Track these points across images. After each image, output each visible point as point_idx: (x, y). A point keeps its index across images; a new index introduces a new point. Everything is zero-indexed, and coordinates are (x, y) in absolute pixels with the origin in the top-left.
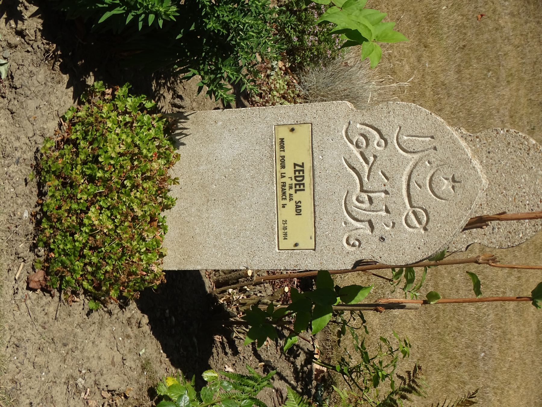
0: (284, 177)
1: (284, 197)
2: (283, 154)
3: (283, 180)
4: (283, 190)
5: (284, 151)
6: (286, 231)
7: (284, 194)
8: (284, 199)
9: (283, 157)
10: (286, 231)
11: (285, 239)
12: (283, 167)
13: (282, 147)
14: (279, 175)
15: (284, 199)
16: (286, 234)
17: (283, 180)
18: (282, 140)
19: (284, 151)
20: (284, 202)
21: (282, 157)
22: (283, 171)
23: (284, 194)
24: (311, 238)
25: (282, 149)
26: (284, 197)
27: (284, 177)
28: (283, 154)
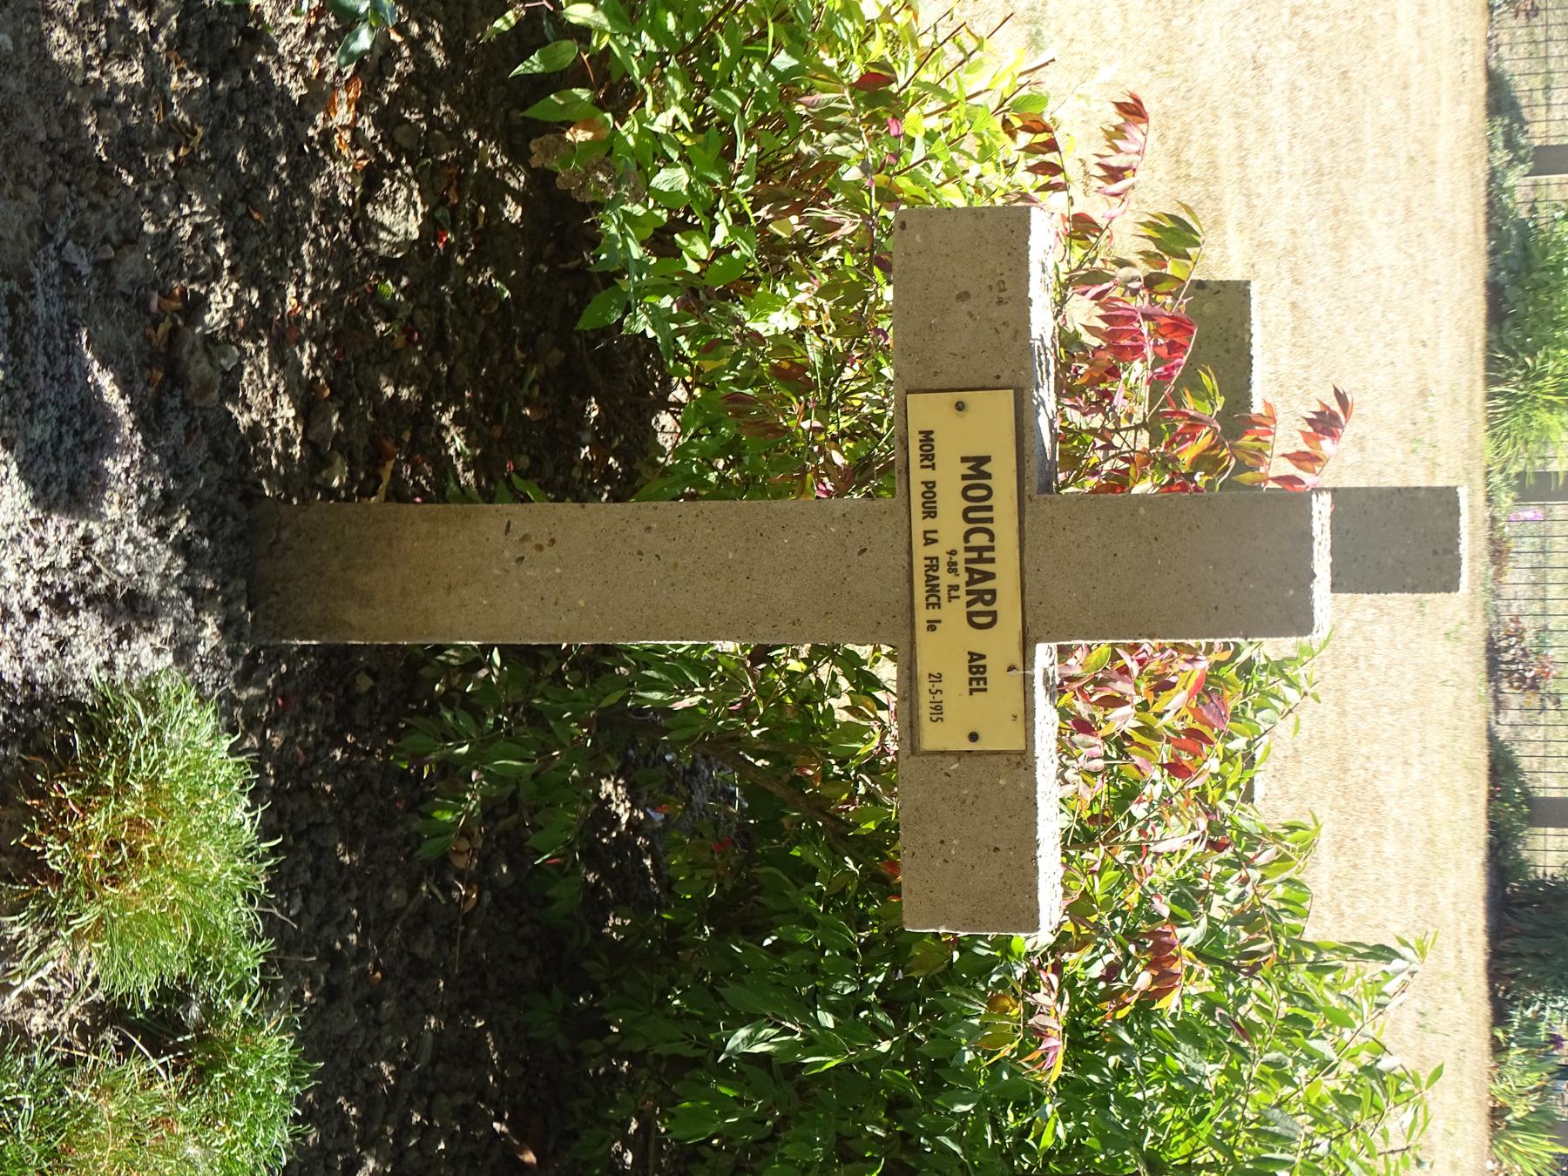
0: (935, 541)
1: (933, 600)
2: (928, 475)
3: (932, 550)
4: (930, 579)
5: (933, 467)
6: (938, 697)
7: (933, 589)
8: (933, 605)
9: (930, 486)
10: (938, 697)
12: (930, 513)
13: (928, 456)
15: (933, 605)
16: (938, 708)
17: (932, 550)
18: (927, 437)
19: (933, 467)
20: (933, 614)
22: (930, 524)
23: (933, 589)
25: (926, 463)
26: (933, 600)
27: (935, 541)
28: (928, 475)
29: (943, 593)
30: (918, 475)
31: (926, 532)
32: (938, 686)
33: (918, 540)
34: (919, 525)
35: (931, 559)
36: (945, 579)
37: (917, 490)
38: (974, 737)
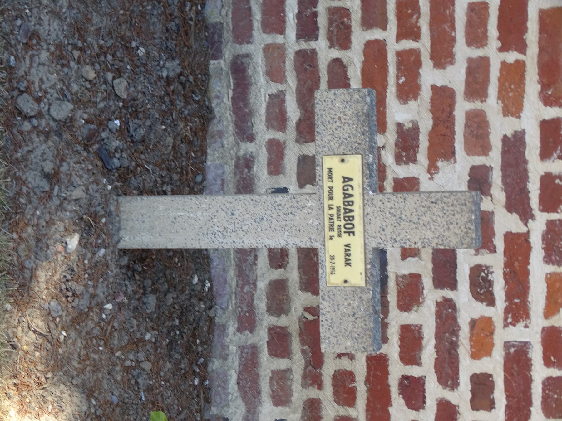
0: (332, 208)
2: (330, 184)
3: (331, 212)
6: (333, 265)
9: (331, 188)
10: (333, 265)
11: (332, 273)
12: (331, 198)
13: (330, 177)
14: (326, 208)
16: (333, 268)
17: (331, 212)
18: (330, 170)
19: (332, 181)
21: (329, 187)
22: (331, 202)
24: (361, 274)
25: (330, 180)
27: (332, 208)
28: (330, 184)
29: (335, 227)
30: (327, 185)
31: (329, 205)
32: (333, 261)
33: (326, 208)
34: (326, 202)
35: (330, 215)
36: (336, 223)
37: (326, 189)
38: (346, 281)
